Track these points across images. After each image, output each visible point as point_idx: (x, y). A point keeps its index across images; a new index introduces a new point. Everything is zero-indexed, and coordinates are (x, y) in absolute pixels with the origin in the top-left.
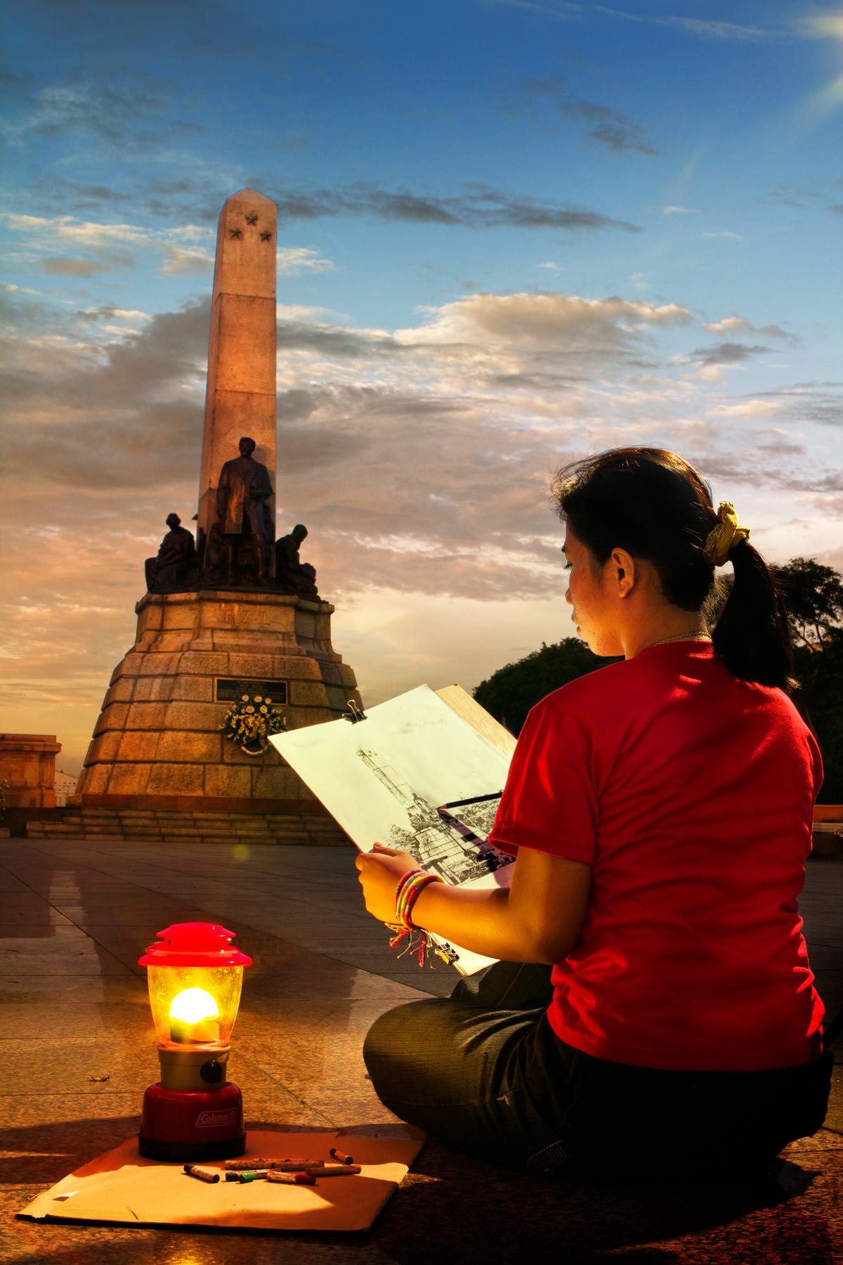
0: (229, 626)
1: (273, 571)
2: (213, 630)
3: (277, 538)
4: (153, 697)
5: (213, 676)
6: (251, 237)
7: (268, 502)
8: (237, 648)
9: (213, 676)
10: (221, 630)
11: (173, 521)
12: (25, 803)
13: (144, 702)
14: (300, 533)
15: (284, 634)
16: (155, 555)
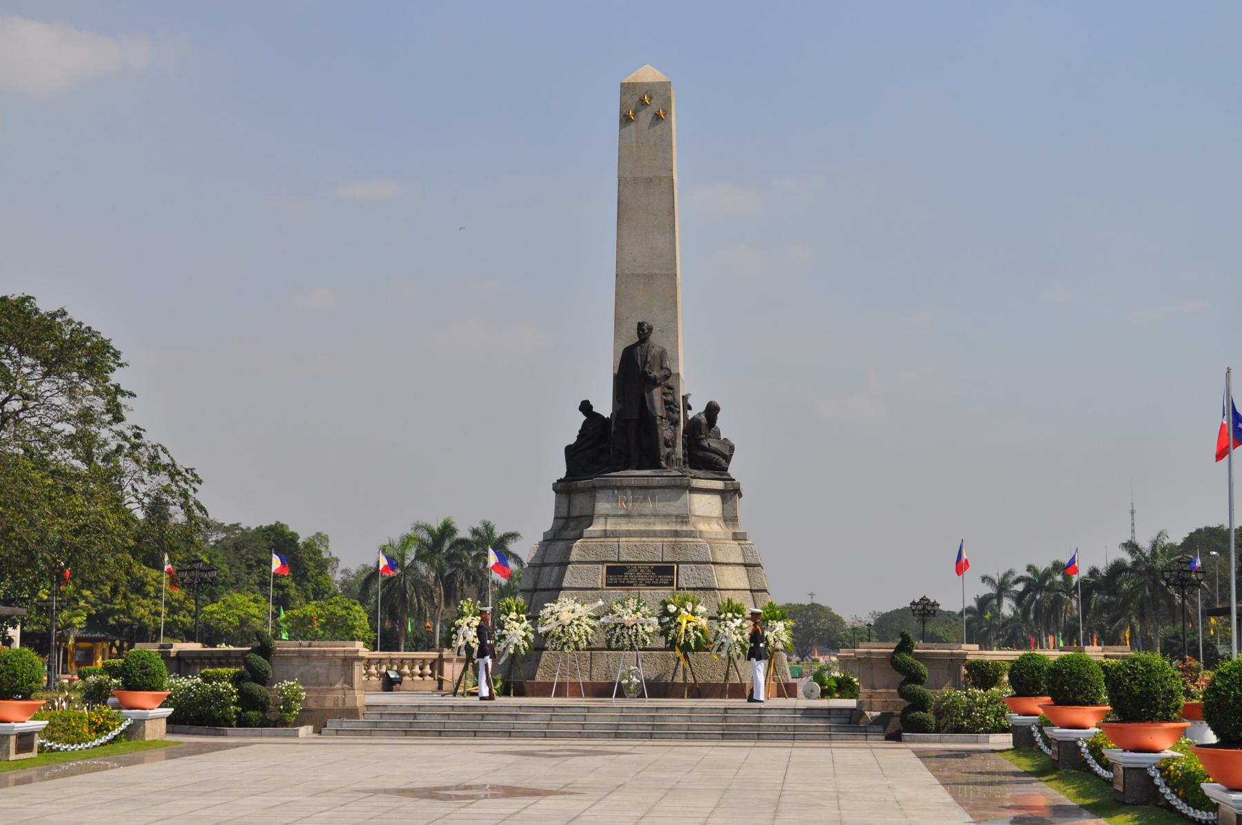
0: (622, 512)
1: (679, 449)
2: (606, 516)
3: (691, 414)
4: (551, 585)
5: (602, 562)
6: (645, 117)
7: (670, 382)
8: (629, 534)
9: (602, 562)
10: (615, 516)
11: (586, 407)
12: (329, 704)
13: (545, 590)
14: (712, 411)
15: (677, 517)
16: (572, 439)
